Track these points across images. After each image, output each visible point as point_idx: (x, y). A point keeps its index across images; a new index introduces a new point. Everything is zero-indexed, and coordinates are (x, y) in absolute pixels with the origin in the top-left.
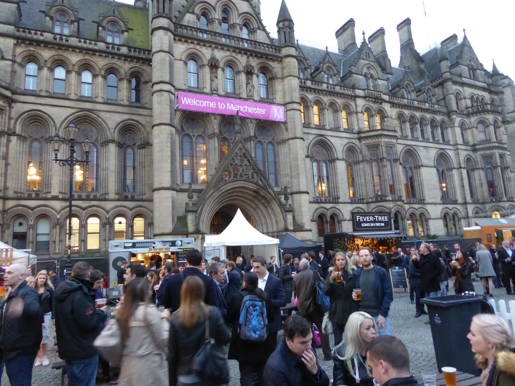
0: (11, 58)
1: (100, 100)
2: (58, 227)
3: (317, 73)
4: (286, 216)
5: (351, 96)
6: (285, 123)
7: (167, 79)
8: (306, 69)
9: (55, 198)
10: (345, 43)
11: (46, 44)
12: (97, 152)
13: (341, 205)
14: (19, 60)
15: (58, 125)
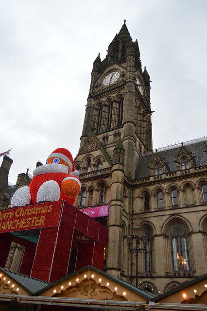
6: (108, 216)
12: (186, 241)
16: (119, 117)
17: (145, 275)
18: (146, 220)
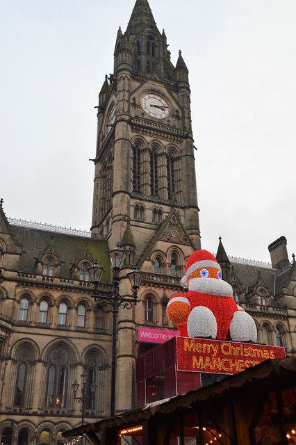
0: (13, 297)
1: (72, 328)
2: (35, 440)
3: (251, 295)
5: (284, 316)
7: (131, 318)
8: (240, 293)
9: (35, 414)
10: (278, 258)
11: (37, 285)
14: (17, 298)
15: (41, 351)
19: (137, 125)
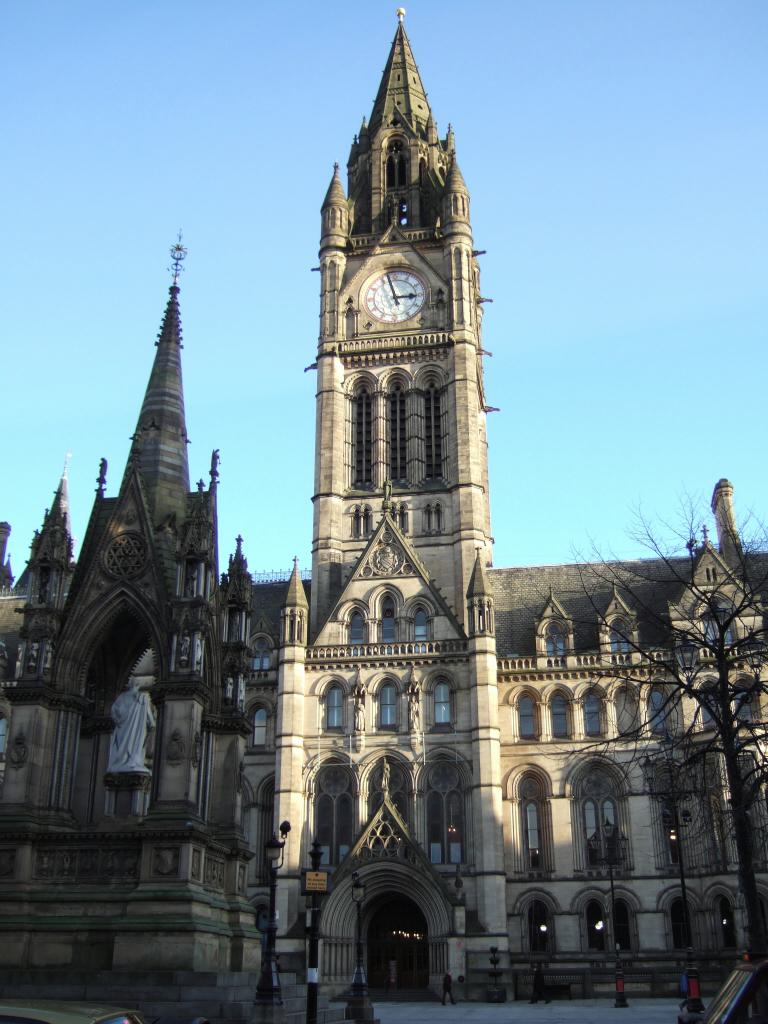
4: (453, 912)
13: (634, 881)
16: (429, 447)
17: (526, 876)
18: (531, 760)
19: (352, 354)
